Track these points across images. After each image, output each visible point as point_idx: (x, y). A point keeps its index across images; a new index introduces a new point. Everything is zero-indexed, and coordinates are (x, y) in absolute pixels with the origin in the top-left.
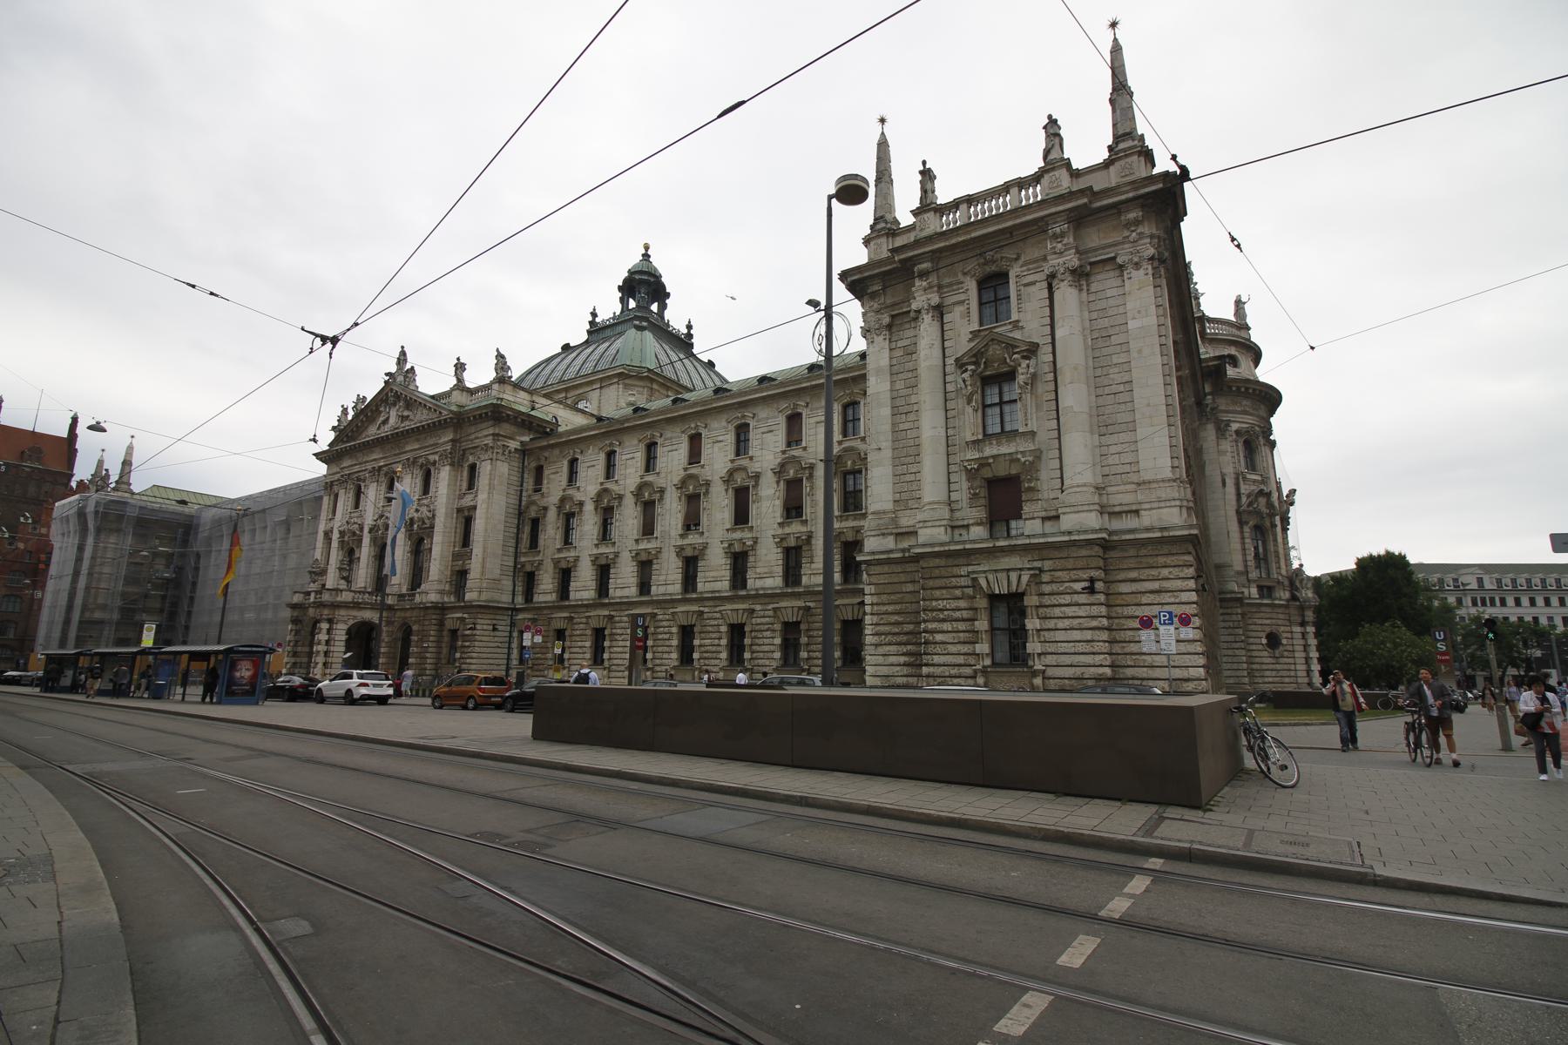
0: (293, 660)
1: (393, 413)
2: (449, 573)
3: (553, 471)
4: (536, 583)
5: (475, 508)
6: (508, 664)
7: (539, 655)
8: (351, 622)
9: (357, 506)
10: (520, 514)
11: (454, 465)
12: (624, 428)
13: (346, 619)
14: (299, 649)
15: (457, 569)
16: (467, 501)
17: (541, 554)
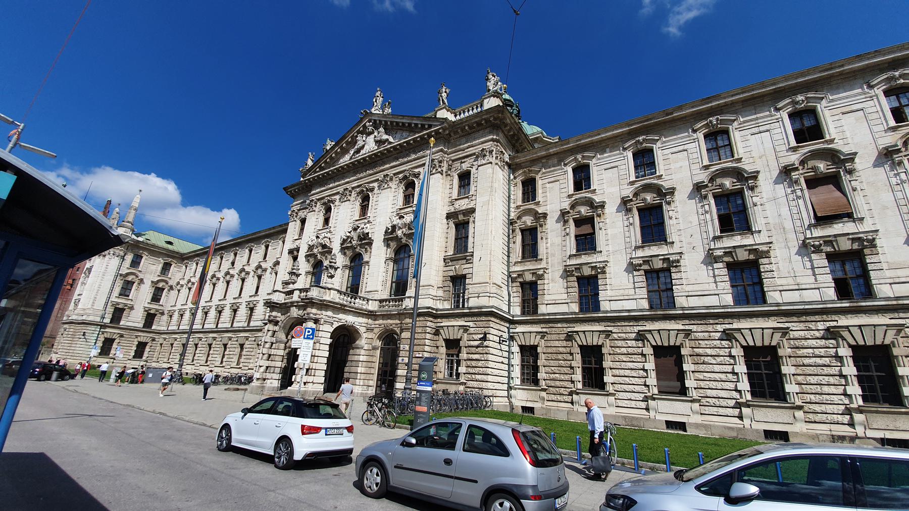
0: (267, 363)
1: (371, 139)
2: (441, 278)
3: (552, 179)
4: (540, 292)
5: (473, 211)
6: (508, 384)
7: (557, 375)
8: (336, 325)
9: (327, 221)
10: (511, 223)
11: (442, 174)
12: (674, 120)
13: (331, 320)
14: (273, 352)
15: (451, 274)
16: (463, 205)
17: (544, 262)
